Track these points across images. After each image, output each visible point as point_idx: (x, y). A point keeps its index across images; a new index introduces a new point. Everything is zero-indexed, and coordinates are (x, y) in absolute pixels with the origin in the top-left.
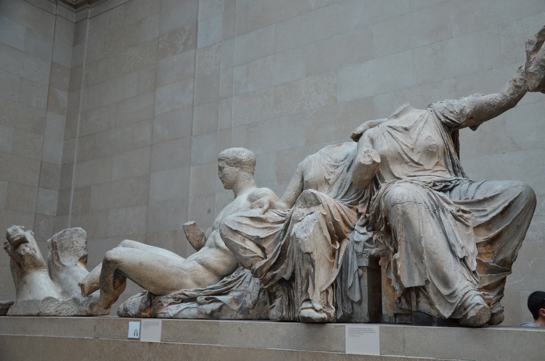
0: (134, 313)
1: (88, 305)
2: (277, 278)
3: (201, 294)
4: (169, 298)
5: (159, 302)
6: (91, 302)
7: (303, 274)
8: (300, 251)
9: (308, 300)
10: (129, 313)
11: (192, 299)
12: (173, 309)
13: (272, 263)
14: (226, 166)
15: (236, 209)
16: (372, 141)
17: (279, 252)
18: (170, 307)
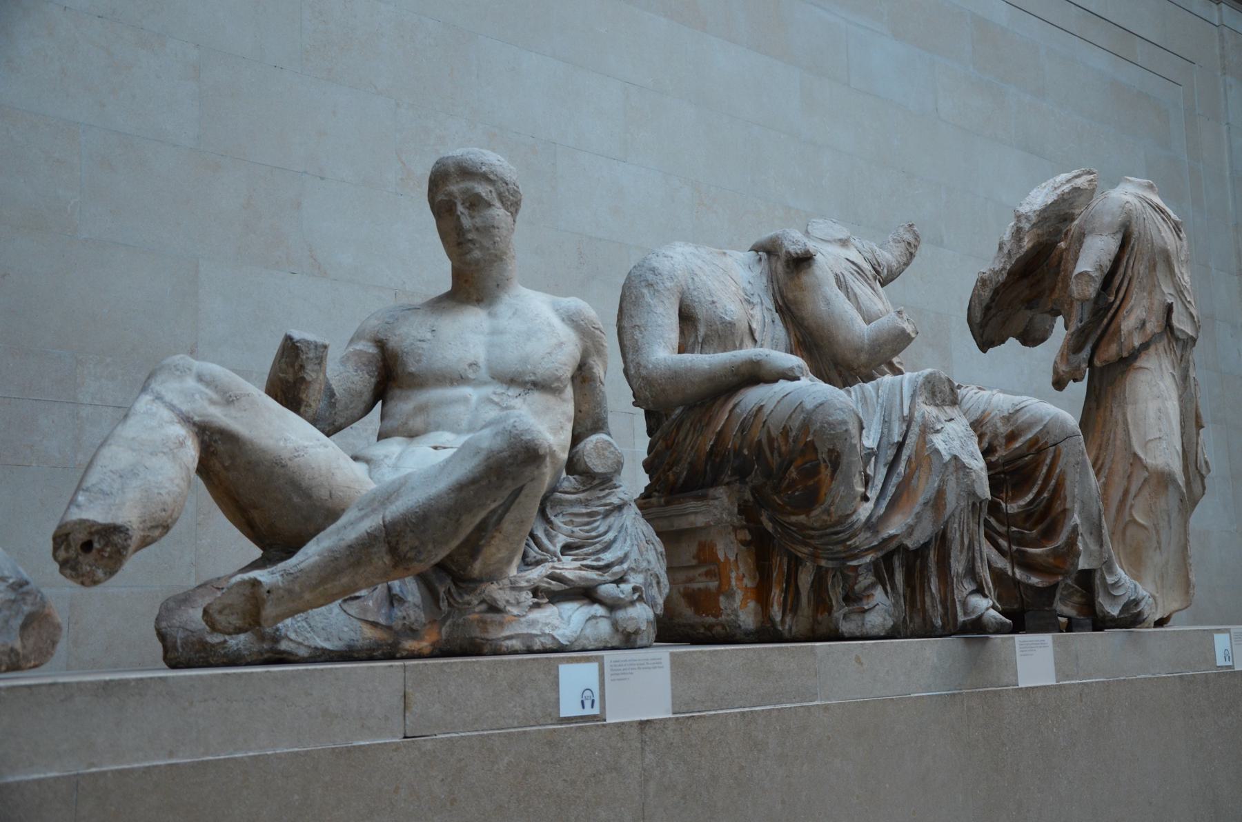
0: (321, 643)
1: (17, 622)
2: (893, 545)
3: (607, 577)
4: (521, 589)
5: (483, 601)
6: (27, 609)
7: (966, 542)
8: (972, 494)
9: (980, 591)
10: (284, 646)
11: (587, 594)
12: (556, 622)
13: (882, 511)
14: (498, 204)
15: (554, 341)
16: (840, 282)
17: (891, 490)
18: (536, 615)
